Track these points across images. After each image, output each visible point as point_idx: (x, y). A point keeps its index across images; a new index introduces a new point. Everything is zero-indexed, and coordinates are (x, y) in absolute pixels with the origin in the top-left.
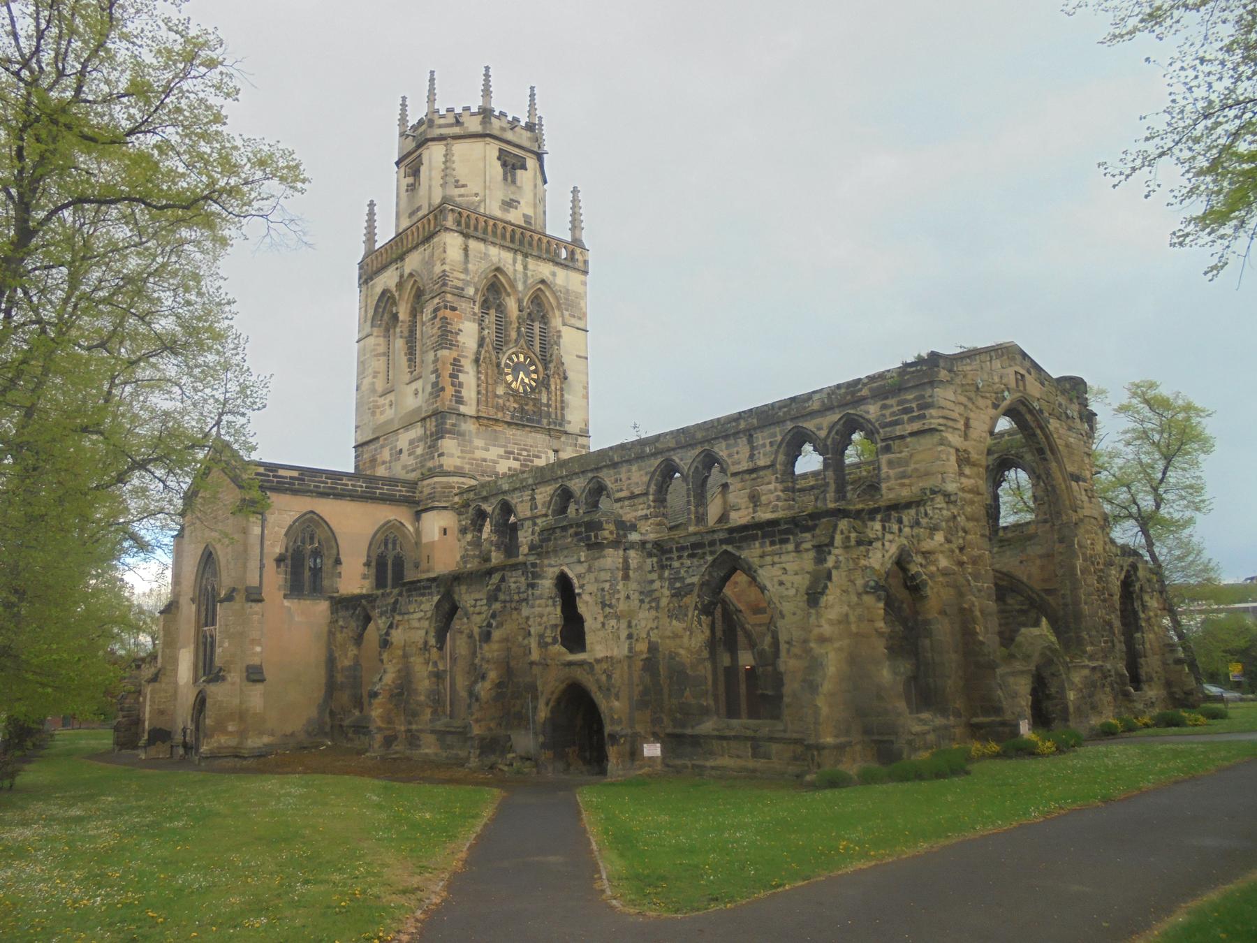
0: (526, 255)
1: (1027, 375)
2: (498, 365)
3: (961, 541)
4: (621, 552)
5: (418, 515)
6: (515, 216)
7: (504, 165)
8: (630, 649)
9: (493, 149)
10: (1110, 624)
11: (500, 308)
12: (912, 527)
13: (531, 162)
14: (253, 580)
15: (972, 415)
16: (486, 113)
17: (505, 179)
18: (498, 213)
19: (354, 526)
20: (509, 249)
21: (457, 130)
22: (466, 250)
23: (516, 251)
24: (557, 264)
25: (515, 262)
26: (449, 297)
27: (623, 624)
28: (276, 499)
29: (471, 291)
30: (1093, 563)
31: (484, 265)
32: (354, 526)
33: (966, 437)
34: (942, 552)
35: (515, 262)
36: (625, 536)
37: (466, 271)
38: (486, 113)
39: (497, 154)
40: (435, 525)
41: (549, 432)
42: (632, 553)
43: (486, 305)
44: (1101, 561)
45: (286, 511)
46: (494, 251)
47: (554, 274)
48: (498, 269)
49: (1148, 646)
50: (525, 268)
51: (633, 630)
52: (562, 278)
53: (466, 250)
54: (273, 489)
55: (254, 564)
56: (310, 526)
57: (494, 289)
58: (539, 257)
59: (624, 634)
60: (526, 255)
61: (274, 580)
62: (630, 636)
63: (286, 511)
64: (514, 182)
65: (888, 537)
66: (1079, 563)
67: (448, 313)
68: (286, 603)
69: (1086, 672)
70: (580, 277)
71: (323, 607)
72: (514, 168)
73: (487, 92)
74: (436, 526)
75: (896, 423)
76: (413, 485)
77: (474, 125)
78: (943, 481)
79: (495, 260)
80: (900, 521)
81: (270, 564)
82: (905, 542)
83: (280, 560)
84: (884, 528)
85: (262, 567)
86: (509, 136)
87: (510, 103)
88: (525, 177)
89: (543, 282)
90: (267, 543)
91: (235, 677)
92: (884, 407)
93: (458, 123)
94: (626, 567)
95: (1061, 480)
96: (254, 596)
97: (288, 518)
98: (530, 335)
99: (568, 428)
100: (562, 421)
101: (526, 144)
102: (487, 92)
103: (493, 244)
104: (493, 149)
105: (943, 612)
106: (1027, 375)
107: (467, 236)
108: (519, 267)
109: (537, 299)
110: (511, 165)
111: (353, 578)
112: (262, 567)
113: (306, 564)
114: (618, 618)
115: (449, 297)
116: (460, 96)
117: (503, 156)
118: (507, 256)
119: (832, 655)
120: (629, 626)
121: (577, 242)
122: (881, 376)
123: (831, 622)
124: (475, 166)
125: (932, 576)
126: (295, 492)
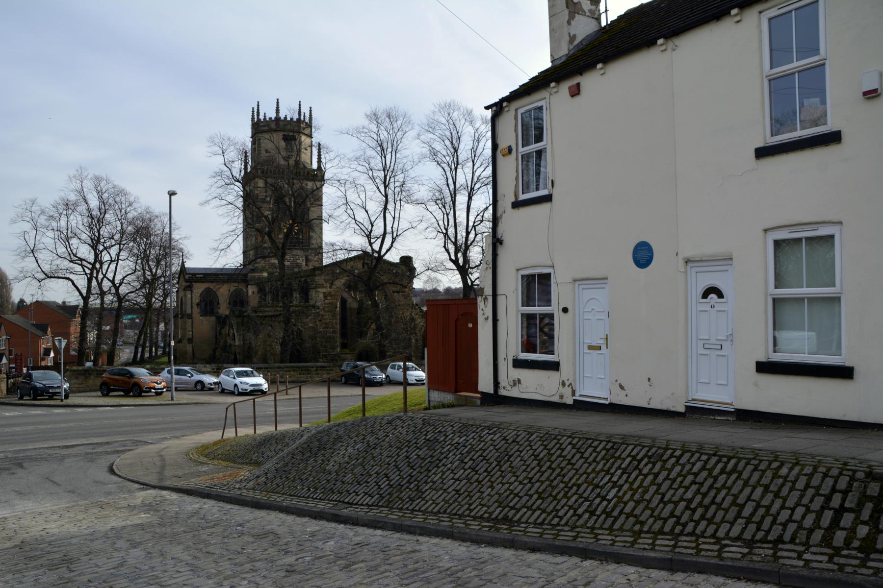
5: (247, 287)
14: (189, 311)
16: (278, 119)
19: (224, 292)
28: (195, 285)
29: (268, 199)
32: (224, 292)
38: (278, 119)
39: (281, 137)
40: (251, 290)
41: (302, 250)
45: (199, 289)
52: (310, 185)
55: (189, 307)
56: (208, 291)
61: (196, 311)
63: (199, 289)
71: (213, 318)
72: (291, 140)
73: (278, 111)
74: (251, 290)
76: (246, 275)
81: (195, 306)
83: (198, 304)
87: (288, 112)
91: (185, 341)
96: (190, 316)
97: (200, 291)
99: (312, 246)
100: (309, 244)
102: (278, 111)
111: (224, 309)
112: (192, 307)
113: (208, 304)
117: (286, 139)
121: (319, 167)
124: (274, 143)
126: (202, 282)
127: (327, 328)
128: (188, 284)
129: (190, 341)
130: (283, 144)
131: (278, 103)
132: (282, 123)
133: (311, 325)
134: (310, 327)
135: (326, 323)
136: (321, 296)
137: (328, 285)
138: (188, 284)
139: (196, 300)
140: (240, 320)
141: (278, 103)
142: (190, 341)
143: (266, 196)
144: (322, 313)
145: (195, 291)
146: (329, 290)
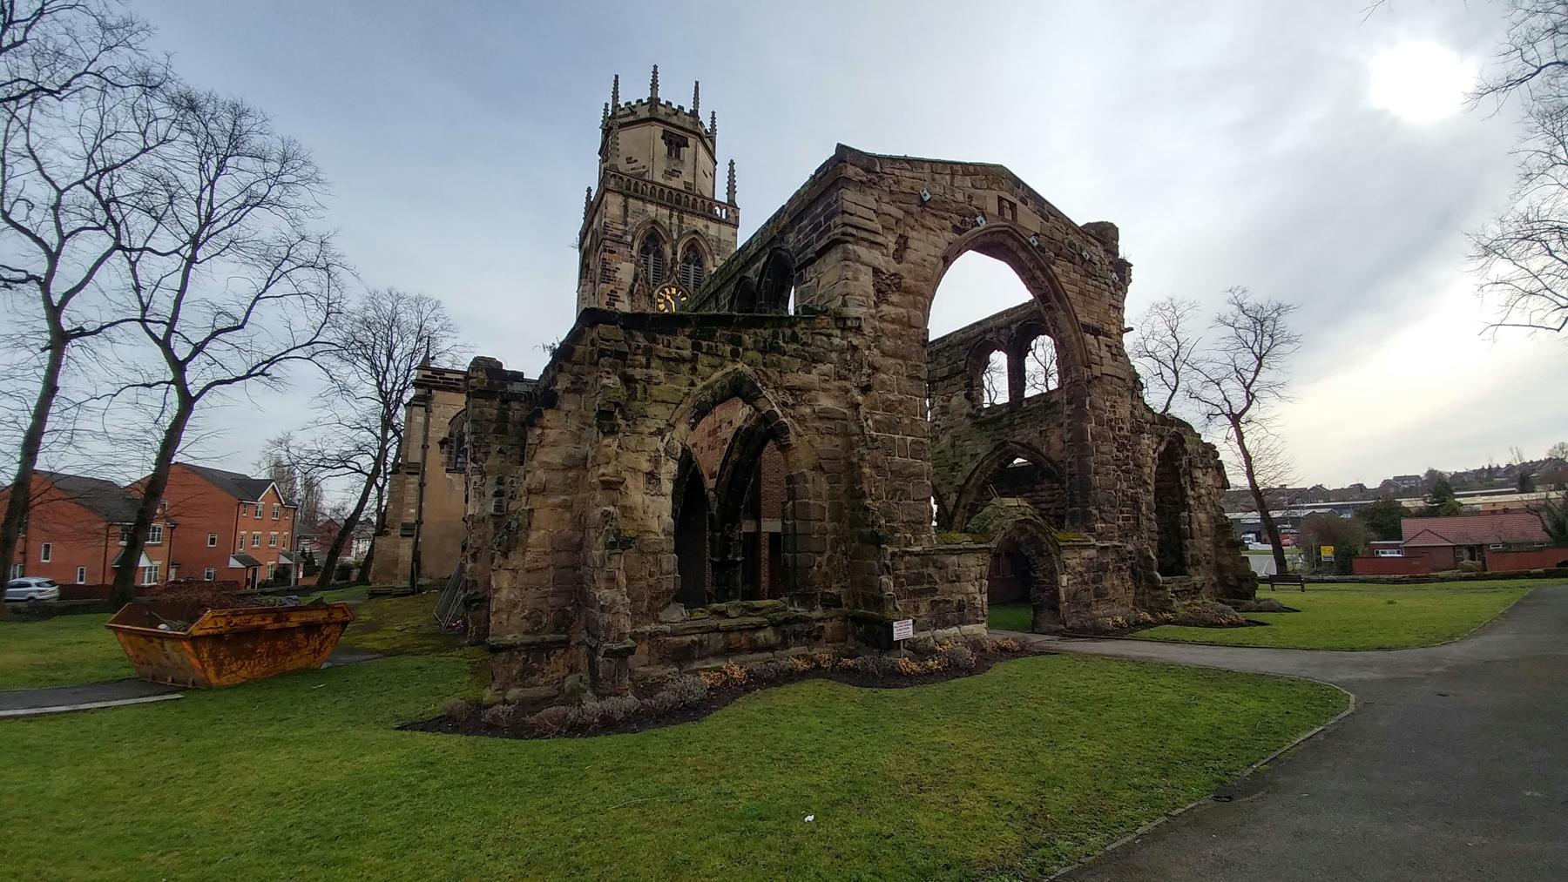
0: (681, 212)
1: (1019, 204)
2: (651, 296)
3: (864, 379)
4: (496, 403)
6: (676, 183)
7: (669, 143)
8: (498, 507)
9: (657, 130)
10: (1135, 500)
11: (659, 254)
12: (763, 352)
13: (691, 141)
14: (415, 456)
15: (912, 234)
16: (654, 101)
17: (670, 154)
18: (661, 181)
20: (666, 206)
21: (631, 118)
22: (626, 207)
23: (672, 209)
24: (711, 219)
25: (671, 217)
26: (608, 243)
27: (491, 480)
28: (438, 395)
29: (629, 238)
30: (1112, 429)
31: (641, 219)
33: (899, 256)
34: (824, 390)
35: (671, 217)
36: (504, 386)
37: (626, 224)
38: (654, 101)
42: (515, 405)
43: (644, 250)
44: (1127, 426)
46: (651, 209)
47: (707, 227)
48: (654, 222)
49: (1195, 526)
50: (681, 220)
51: (506, 488)
53: (626, 207)
54: (437, 388)
57: (652, 240)
58: (693, 214)
59: (490, 492)
60: (681, 212)
61: (436, 457)
62: (499, 494)
64: (678, 156)
65: (704, 359)
66: (1091, 427)
67: (607, 255)
68: (448, 476)
69: (1092, 553)
70: (730, 229)
72: (679, 146)
73: (654, 85)
75: (807, 246)
77: (644, 113)
78: (845, 304)
79: (653, 215)
80: (736, 341)
81: (434, 448)
82: (748, 370)
83: (443, 443)
84: (696, 347)
85: (425, 447)
86: (674, 120)
87: (675, 94)
88: (686, 153)
89: (696, 232)
90: (432, 430)
92: (799, 232)
93: (633, 113)
94: (503, 419)
95: (1071, 331)
98: (687, 275)
101: (688, 126)
102: (654, 85)
103: (652, 202)
104: (657, 130)
105: (818, 468)
106: (1019, 204)
107: (627, 196)
108: (675, 220)
109: (692, 247)
110: (675, 143)
112: (425, 447)
114: (483, 474)
115: (608, 243)
116: (634, 92)
117: (666, 136)
118: (666, 212)
119: (541, 516)
120: (500, 482)
121: (731, 204)
122: (798, 193)
123: (548, 467)
124: (646, 145)
125: (801, 420)
127: (891, 427)
128: (421, 391)
129: (409, 530)
130: (662, 147)
131: (655, 73)
132: (662, 110)
133: (826, 402)
134: (825, 416)
135: (889, 407)
136: (866, 280)
137: (891, 240)
138: (421, 391)
139: (439, 431)
140: (491, 410)
141: (655, 73)
142: (409, 530)
143: (625, 233)
144: (874, 355)
145: (436, 411)
146: (893, 267)
